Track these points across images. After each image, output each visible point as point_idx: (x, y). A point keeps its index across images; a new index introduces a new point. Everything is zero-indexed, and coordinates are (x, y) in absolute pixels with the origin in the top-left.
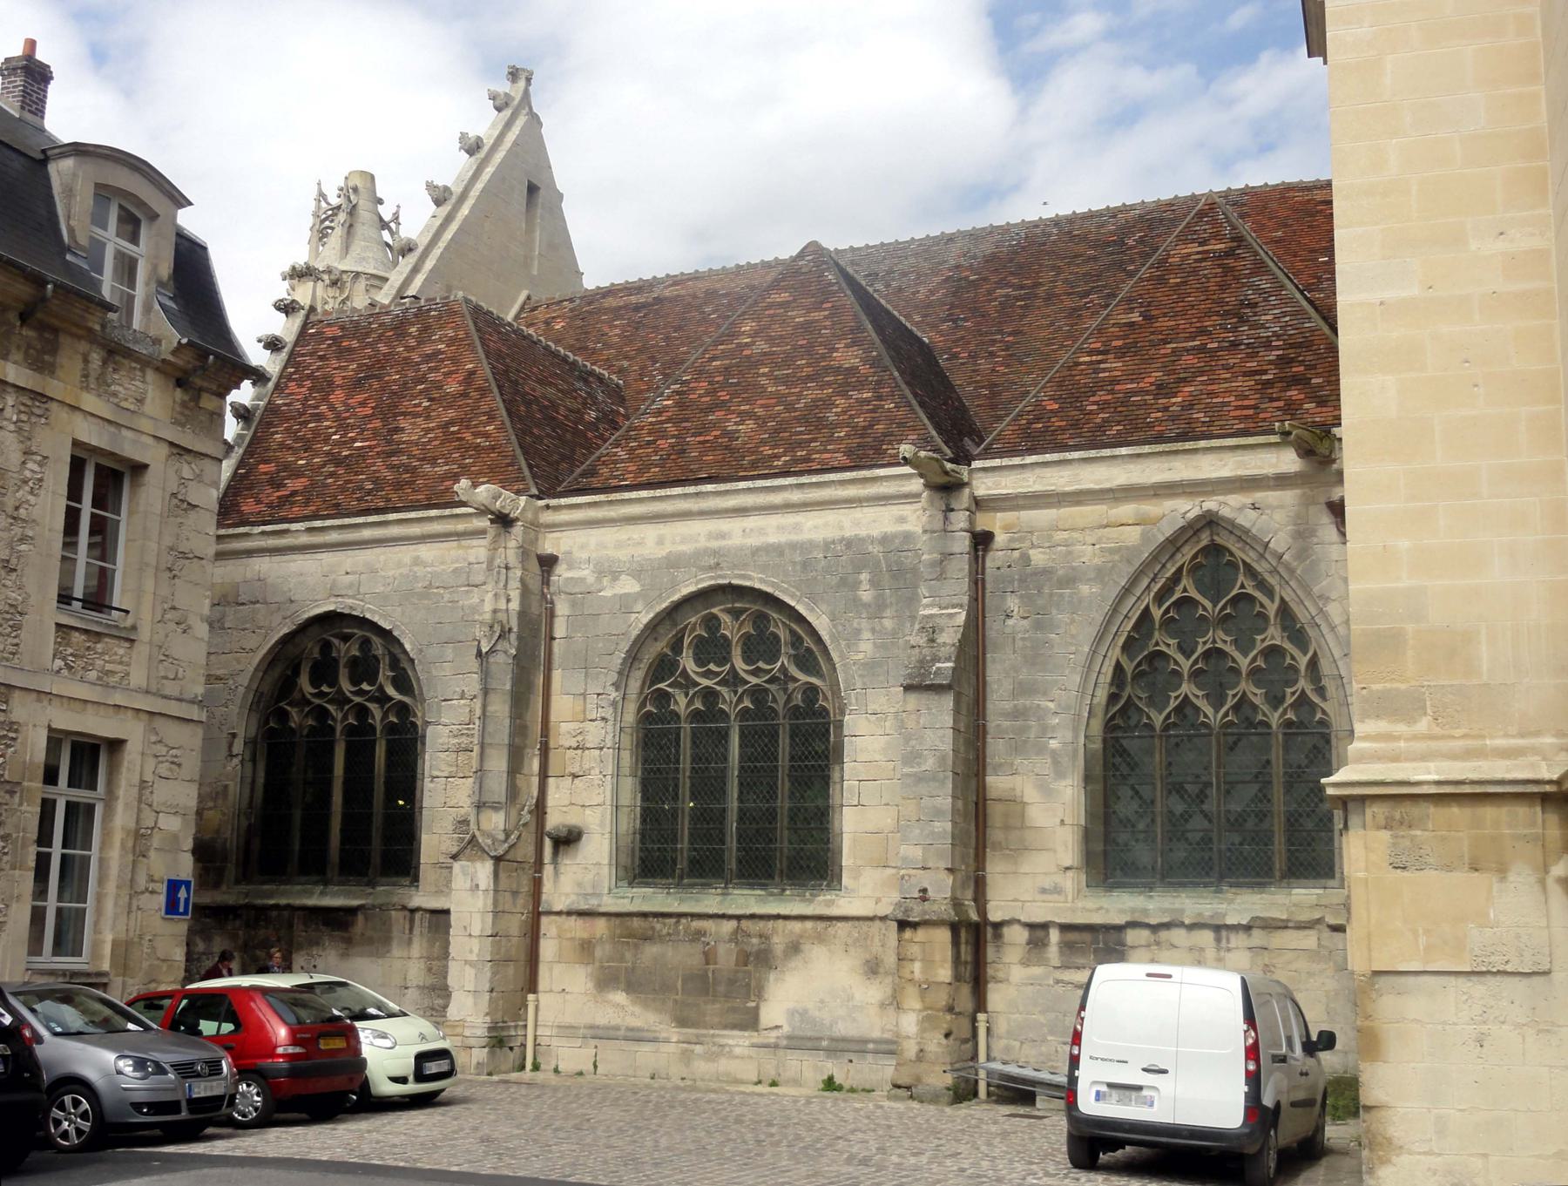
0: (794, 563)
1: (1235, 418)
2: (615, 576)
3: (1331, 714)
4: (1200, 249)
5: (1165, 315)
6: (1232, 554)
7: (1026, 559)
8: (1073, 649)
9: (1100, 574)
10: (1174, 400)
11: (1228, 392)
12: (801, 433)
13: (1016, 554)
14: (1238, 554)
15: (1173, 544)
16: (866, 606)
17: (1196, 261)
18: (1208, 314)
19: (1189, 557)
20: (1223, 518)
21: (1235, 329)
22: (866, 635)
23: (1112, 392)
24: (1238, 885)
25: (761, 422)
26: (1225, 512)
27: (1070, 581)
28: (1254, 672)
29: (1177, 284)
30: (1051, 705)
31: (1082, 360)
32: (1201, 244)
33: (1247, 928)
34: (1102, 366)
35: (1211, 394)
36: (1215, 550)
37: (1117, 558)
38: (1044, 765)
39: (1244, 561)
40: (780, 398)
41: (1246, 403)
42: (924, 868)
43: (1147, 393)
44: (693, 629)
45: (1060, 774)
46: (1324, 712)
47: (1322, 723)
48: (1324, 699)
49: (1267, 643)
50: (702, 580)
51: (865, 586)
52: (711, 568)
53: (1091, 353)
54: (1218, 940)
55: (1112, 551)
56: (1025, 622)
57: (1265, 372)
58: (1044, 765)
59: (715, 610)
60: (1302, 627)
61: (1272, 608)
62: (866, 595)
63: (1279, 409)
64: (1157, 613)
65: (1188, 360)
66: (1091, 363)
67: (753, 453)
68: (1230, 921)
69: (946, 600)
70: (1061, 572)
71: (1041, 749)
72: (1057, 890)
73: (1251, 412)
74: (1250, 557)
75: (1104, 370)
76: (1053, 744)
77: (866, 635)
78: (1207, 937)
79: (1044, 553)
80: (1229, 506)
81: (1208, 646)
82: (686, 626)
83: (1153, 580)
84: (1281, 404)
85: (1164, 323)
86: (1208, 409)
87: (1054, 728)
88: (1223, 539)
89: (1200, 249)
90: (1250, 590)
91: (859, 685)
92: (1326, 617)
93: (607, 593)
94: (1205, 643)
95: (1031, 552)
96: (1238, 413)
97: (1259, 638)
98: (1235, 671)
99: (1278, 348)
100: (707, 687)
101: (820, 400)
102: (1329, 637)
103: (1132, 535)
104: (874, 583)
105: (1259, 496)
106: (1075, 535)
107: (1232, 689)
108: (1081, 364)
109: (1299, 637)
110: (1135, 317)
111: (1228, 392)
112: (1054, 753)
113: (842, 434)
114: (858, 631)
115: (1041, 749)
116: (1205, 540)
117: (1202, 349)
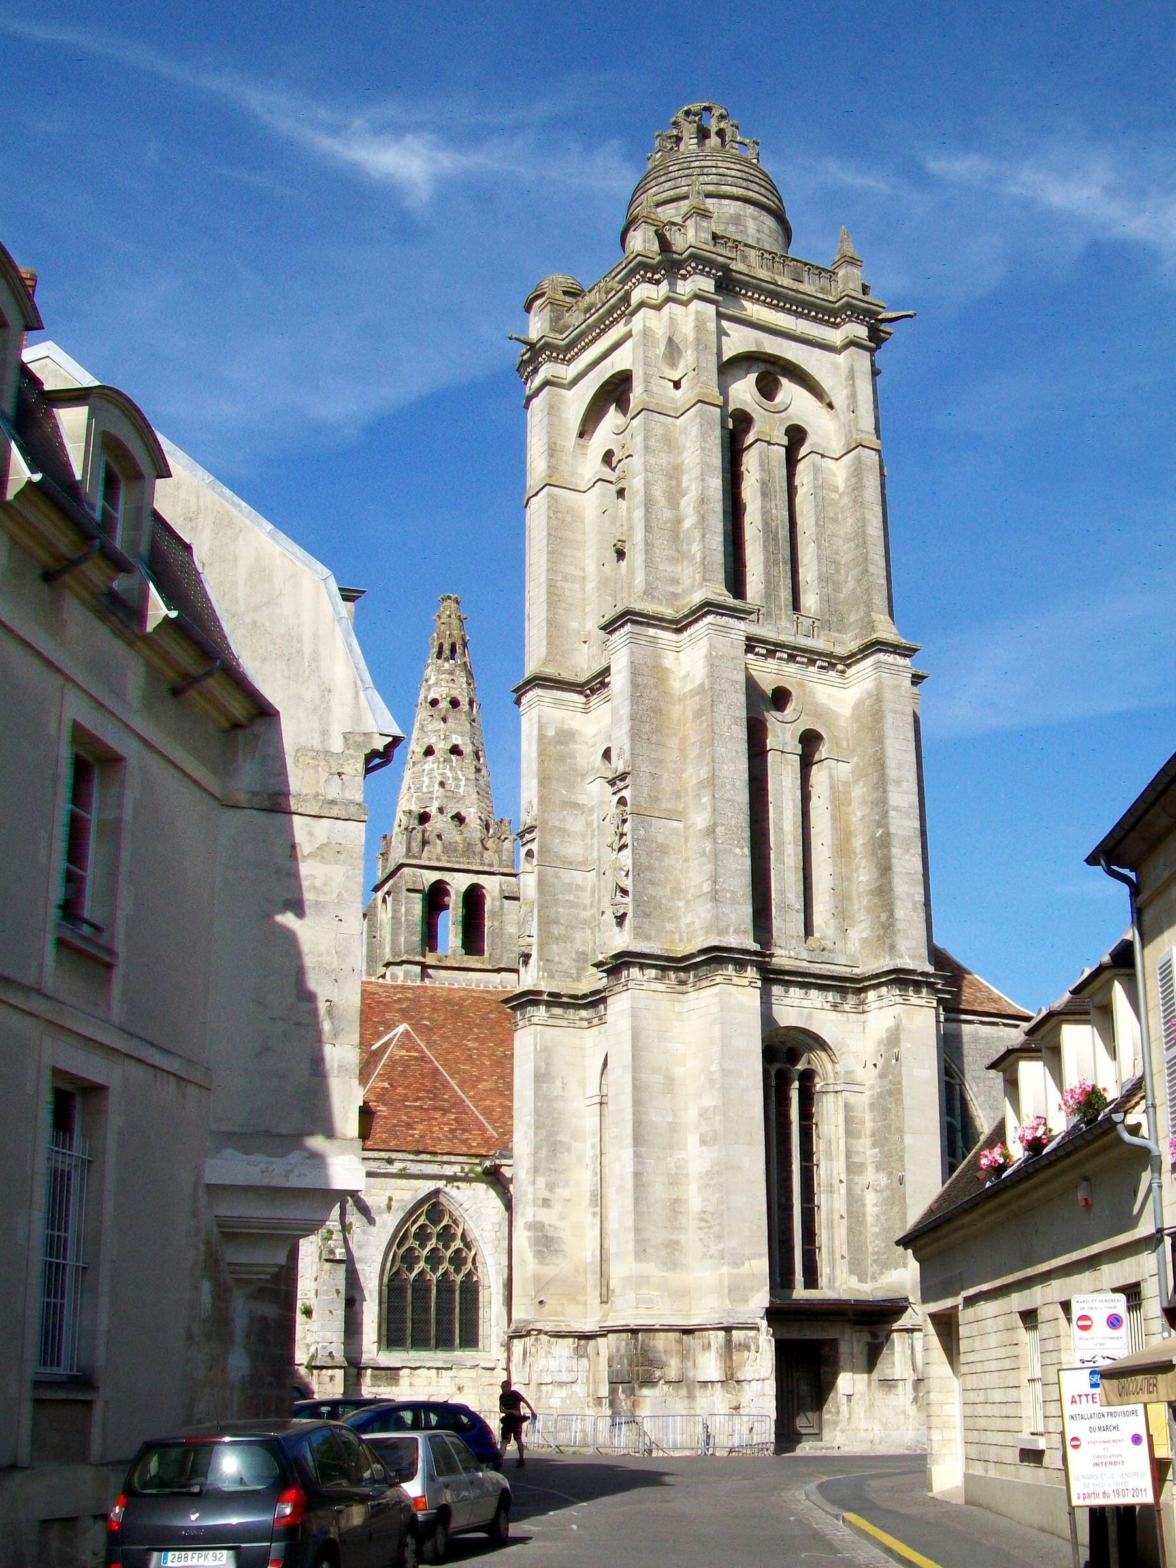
5: (400, 1086)
15: (421, 1202)
18: (419, 1090)
32: (407, 1051)
43: (402, 1126)
54: (438, 1373)
57: (451, 1124)
74: (452, 1208)
78: (434, 1371)
81: (433, 1246)
85: (400, 1090)
90: (451, 1223)
99: (454, 1113)
109: (468, 1245)
110: (386, 1085)
117: (421, 1107)
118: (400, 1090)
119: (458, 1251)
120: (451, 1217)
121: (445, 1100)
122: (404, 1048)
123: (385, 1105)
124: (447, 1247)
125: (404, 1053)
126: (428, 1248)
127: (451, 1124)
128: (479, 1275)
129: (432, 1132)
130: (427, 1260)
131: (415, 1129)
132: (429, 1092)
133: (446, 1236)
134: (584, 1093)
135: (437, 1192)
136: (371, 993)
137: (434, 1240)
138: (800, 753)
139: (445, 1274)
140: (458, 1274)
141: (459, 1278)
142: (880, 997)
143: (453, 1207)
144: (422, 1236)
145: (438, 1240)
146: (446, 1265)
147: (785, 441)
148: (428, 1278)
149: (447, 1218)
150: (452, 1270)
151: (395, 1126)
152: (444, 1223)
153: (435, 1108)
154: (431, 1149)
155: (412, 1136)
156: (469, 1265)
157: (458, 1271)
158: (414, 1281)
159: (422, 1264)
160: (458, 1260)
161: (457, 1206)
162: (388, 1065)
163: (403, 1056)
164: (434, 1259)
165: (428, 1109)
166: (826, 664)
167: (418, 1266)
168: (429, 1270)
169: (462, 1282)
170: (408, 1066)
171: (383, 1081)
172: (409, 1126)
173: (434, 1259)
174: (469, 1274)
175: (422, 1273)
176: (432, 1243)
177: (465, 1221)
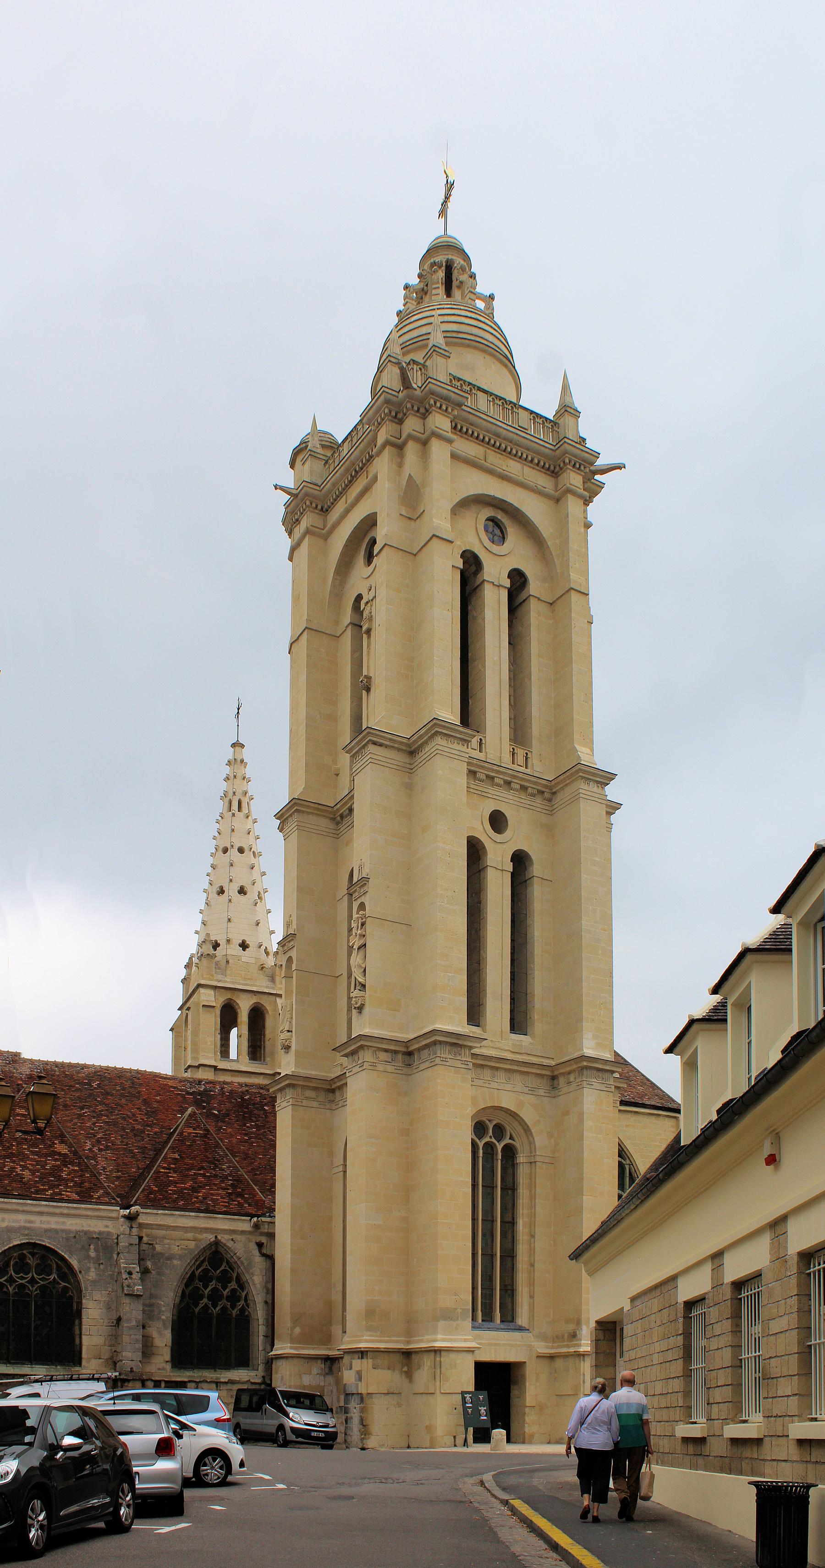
1: (222, 1206)
5: (188, 1157)
6: (222, 1255)
9: (181, 1257)
11: (218, 1194)
14: (224, 1255)
19: (208, 1254)
20: (222, 1243)
23: (175, 1186)
24: (222, 1369)
26: (223, 1241)
28: (228, 1297)
31: (161, 1170)
33: (226, 1383)
35: (212, 1194)
37: (186, 1252)
38: (160, 1325)
41: (225, 1200)
42: (132, 1360)
49: (232, 1287)
53: (164, 1168)
54: (217, 1387)
58: (160, 1325)
60: (243, 1283)
61: (235, 1275)
63: (236, 1205)
64: (197, 1273)
65: (201, 1179)
68: (222, 1380)
71: (159, 1319)
72: (163, 1369)
73: (227, 1204)
75: (171, 1177)
76: (163, 1317)
80: (224, 1238)
81: (214, 1286)
83: (196, 1261)
84: (237, 1203)
86: (212, 1200)
88: (221, 1250)
90: (228, 1269)
92: (253, 1280)
96: (223, 1204)
97: (229, 1285)
98: (222, 1296)
103: (192, 1245)
105: (234, 1237)
107: (220, 1301)
110: (177, 1156)
111: (218, 1194)
112: (163, 1320)
115: (159, 1319)
116: (213, 1248)
119: (234, 1291)
126: (210, 1288)
130: (210, 1297)
131: (199, 1192)
132: (210, 1162)
133: (225, 1279)
134: (332, 1163)
135: (217, 1243)
137: (214, 1282)
138: (512, 871)
139: (224, 1309)
141: (235, 1312)
142: (569, 1083)
143: (229, 1256)
144: (205, 1278)
146: (225, 1301)
147: (507, 583)
149: (224, 1264)
150: (229, 1307)
152: (223, 1268)
156: (242, 1302)
157: (233, 1306)
158: (199, 1313)
159: (205, 1300)
160: (234, 1298)
162: (178, 1140)
164: (215, 1297)
166: (535, 792)
167: (201, 1302)
168: (210, 1306)
170: (195, 1141)
171: (174, 1153)
172: (194, 1190)
173: (215, 1297)
174: (242, 1310)
176: (213, 1284)
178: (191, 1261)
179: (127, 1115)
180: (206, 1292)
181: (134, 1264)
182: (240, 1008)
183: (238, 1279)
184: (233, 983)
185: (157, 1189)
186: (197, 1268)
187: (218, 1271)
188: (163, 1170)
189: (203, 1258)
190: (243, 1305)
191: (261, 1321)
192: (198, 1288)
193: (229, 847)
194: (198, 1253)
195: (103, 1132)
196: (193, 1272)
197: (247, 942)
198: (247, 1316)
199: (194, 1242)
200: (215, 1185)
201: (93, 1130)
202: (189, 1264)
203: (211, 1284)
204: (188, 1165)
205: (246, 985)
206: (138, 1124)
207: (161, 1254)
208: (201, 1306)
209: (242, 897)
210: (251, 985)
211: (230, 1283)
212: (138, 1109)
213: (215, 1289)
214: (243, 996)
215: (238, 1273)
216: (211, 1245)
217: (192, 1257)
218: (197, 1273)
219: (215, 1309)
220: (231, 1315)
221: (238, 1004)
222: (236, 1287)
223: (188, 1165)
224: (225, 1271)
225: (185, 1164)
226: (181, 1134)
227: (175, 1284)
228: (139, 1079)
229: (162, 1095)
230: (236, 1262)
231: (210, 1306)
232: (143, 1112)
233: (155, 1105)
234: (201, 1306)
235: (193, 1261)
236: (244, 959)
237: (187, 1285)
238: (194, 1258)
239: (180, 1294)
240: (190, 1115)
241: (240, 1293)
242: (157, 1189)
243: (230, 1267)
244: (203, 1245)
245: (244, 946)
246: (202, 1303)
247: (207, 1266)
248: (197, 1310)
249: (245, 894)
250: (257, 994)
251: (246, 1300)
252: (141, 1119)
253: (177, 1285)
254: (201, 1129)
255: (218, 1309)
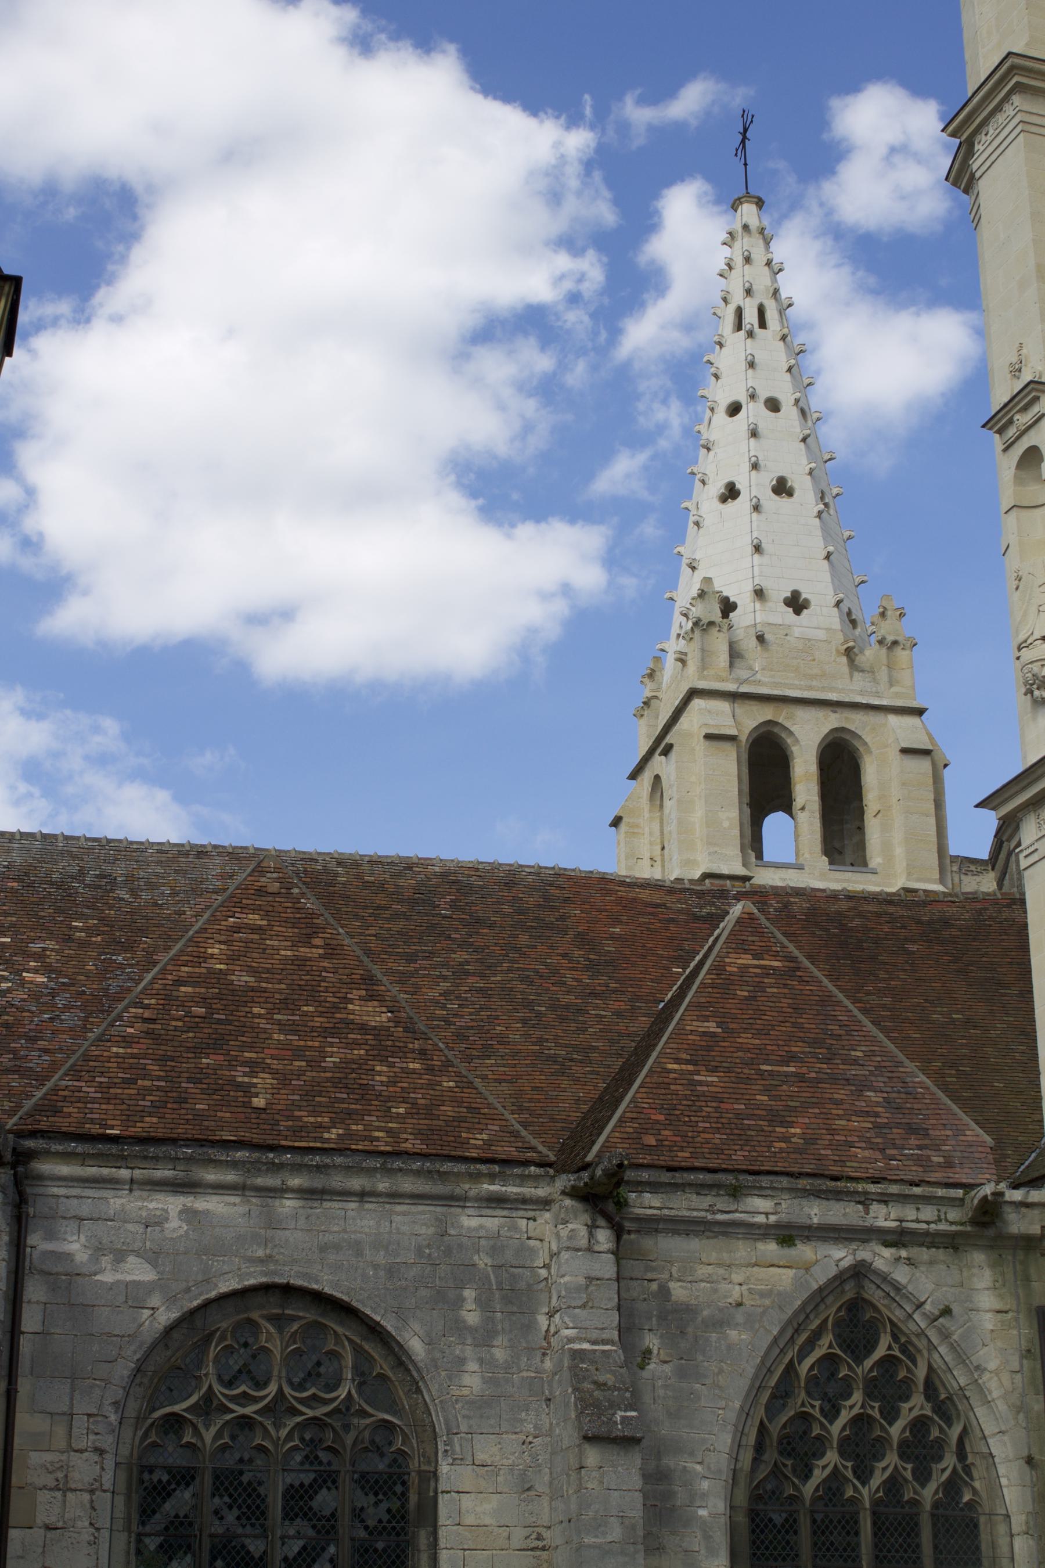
0: (376, 1267)
2: (120, 1256)
3: (984, 1495)
4: (756, 962)
6: (876, 1309)
7: (664, 1292)
8: (723, 1404)
10: (793, 1130)
12: (342, 1101)
13: (654, 1286)
15: (820, 1296)
16: (472, 1330)
17: (757, 975)
21: (828, 1060)
22: (472, 1366)
25: (284, 1079)
26: (879, 1264)
27: (720, 1323)
29: (746, 998)
30: (699, 1468)
31: (670, 1066)
32: (756, 957)
34: (696, 1078)
36: (856, 1306)
39: (889, 1318)
40: (298, 1053)
44: (223, 1338)
45: (712, 1552)
46: (975, 1491)
47: (971, 1505)
48: (972, 1479)
49: (915, 1413)
50: (250, 1275)
51: (470, 1305)
52: (261, 1261)
53: (678, 1061)
55: (762, 1295)
56: (667, 1368)
59: (255, 1315)
60: (949, 1398)
61: (921, 1373)
62: (472, 1317)
66: (682, 1073)
67: (288, 1118)
69: (595, 1335)
70: (705, 1313)
75: (701, 1083)
77: (472, 1366)
79: (686, 1288)
80: (881, 1257)
81: (856, 1410)
82: (218, 1329)
83: (797, 1331)
85: (745, 1039)
87: (704, 1496)
88: (873, 1294)
89: (756, 962)
90: (897, 1353)
91: (463, 1428)
93: (108, 1277)
94: (851, 1407)
95: (672, 1285)
97: (906, 1406)
98: (883, 1442)
100: (244, 1416)
101: (353, 1061)
102: (980, 1412)
104: (484, 1304)
106: (721, 1271)
107: (879, 1461)
108: (670, 1071)
110: (712, 1027)
113: (401, 1110)
114: (462, 1361)
116: (849, 1292)
117: (801, 1078)
118: (745, 1039)
119: (919, 1425)
120: (895, 1338)
121: (855, 1062)
122: (746, 951)
123: (714, 1070)
124: (891, 1415)
125: (746, 960)
126: (844, 1417)
127: (877, 1115)
128: (977, 1484)
129: (832, 1132)
131: (791, 1124)
135: (859, 1272)
136: (647, 904)
137: (857, 1397)
139: (893, 1484)
140: (923, 1485)
141: (929, 1493)
145: (869, 1395)
148: (849, 1493)
149: (885, 1341)
150: (908, 1475)
151: (739, 1116)
152: (880, 1352)
153: (834, 1080)
154: (835, 1170)
155: (786, 1139)
156: (949, 1461)
157: (923, 1476)
158: (815, 1499)
161: (909, 1309)
162: (713, 986)
163: (747, 966)
165: (819, 1081)
167: (821, 1463)
168: (849, 1474)
169: (936, 1505)
171: (706, 1019)
172: (777, 1118)
174: (953, 1486)
175: (835, 1477)
177: (932, 1347)
178: (782, 1331)
179: (536, 971)
180: (836, 1428)
181: (604, 1342)
182: (797, 741)
183: (931, 1389)
184: (776, 685)
185: (662, 1117)
186: (802, 1355)
187: (868, 1363)
188: (676, 1066)
189: (817, 1322)
190: (955, 1469)
191: (1018, 1521)
192: (804, 1417)
193: (743, 398)
194: (805, 1304)
195: (471, 1014)
196: (790, 1368)
197: (803, 596)
198: (971, 1505)
199: (791, 1272)
200: (838, 1103)
201: (444, 1007)
202: (776, 1340)
203: (848, 1403)
204: (748, 1050)
205: (810, 688)
206: (568, 993)
207: (687, 1311)
208: (818, 1475)
209: (783, 501)
210: (823, 689)
211: (907, 1398)
212: (564, 956)
213: (861, 1421)
214: (802, 714)
215: (930, 1368)
216: (841, 1278)
217: (785, 1317)
218: (804, 1368)
219: (863, 1484)
220: (915, 1503)
221: (791, 733)
222: (929, 1413)
223: (748, 1050)
224: (889, 1362)
225: (739, 1049)
226: (719, 969)
227: (737, 1405)
228: (561, 888)
229: (627, 924)
230: (922, 1334)
231: (849, 1474)
232: (578, 962)
233: (609, 945)
234: (818, 1475)
235: (790, 1332)
236: (797, 632)
237: (772, 1410)
238: (789, 1322)
239: (752, 1439)
240: (739, 921)
241: (941, 1430)
242: (662, 1117)
243: (904, 1350)
244: (821, 1277)
245: (796, 603)
246: (824, 1467)
247: (830, 1346)
248: (809, 1489)
249: (790, 493)
250: (839, 710)
251: (961, 1454)
252: (574, 979)
253: (742, 1408)
254: (775, 956)
255: (876, 1481)
